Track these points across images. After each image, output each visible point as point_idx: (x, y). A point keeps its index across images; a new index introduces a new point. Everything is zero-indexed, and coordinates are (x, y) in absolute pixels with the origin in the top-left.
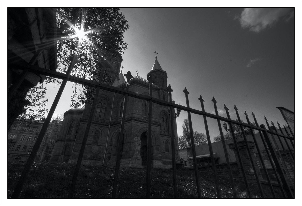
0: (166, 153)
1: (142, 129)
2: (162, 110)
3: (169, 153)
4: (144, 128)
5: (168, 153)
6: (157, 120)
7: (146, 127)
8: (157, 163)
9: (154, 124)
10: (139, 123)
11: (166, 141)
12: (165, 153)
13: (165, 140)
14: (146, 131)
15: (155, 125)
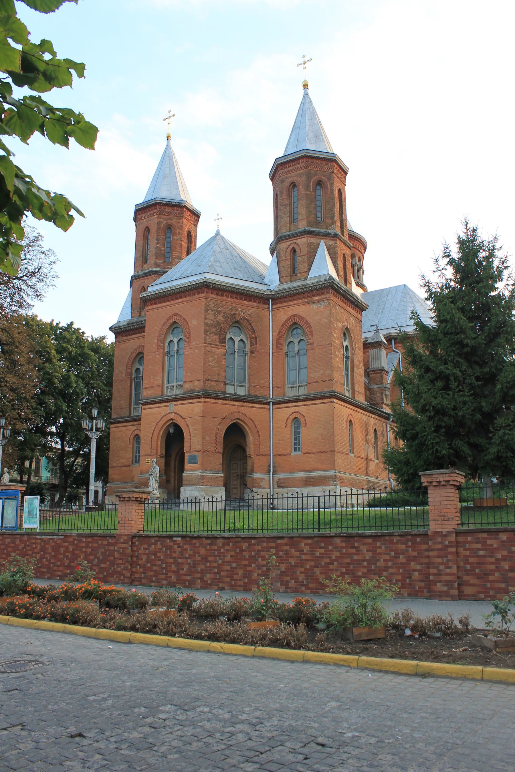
0: (293, 453)
1: (161, 419)
2: (286, 319)
3: (304, 454)
4: (165, 416)
5: (300, 453)
6: (196, 383)
7: (169, 413)
8: (188, 492)
9: (188, 399)
10: (155, 408)
11: (296, 418)
12: (289, 455)
13: (292, 417)
14: (171, 422)
15: (190, 401)
